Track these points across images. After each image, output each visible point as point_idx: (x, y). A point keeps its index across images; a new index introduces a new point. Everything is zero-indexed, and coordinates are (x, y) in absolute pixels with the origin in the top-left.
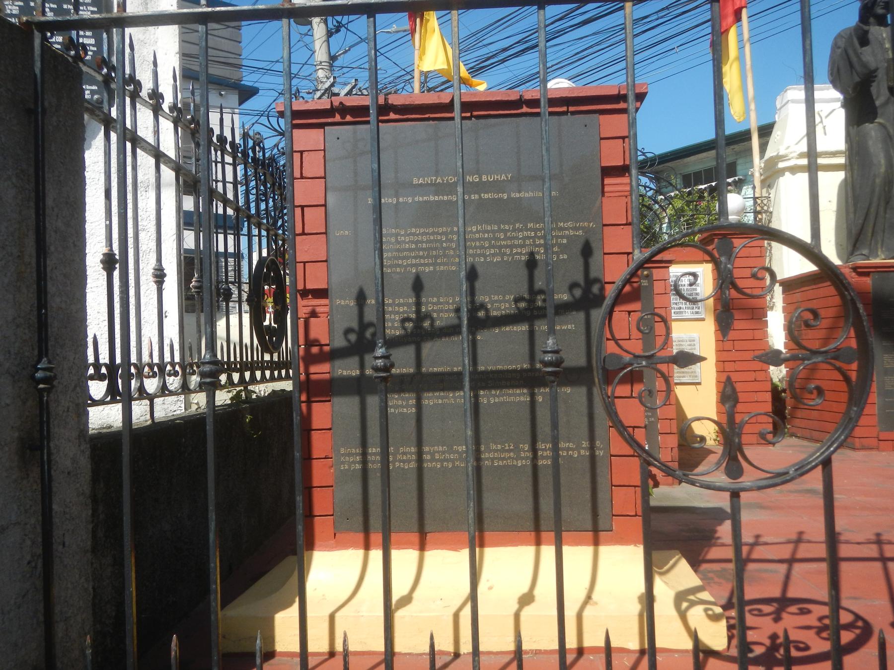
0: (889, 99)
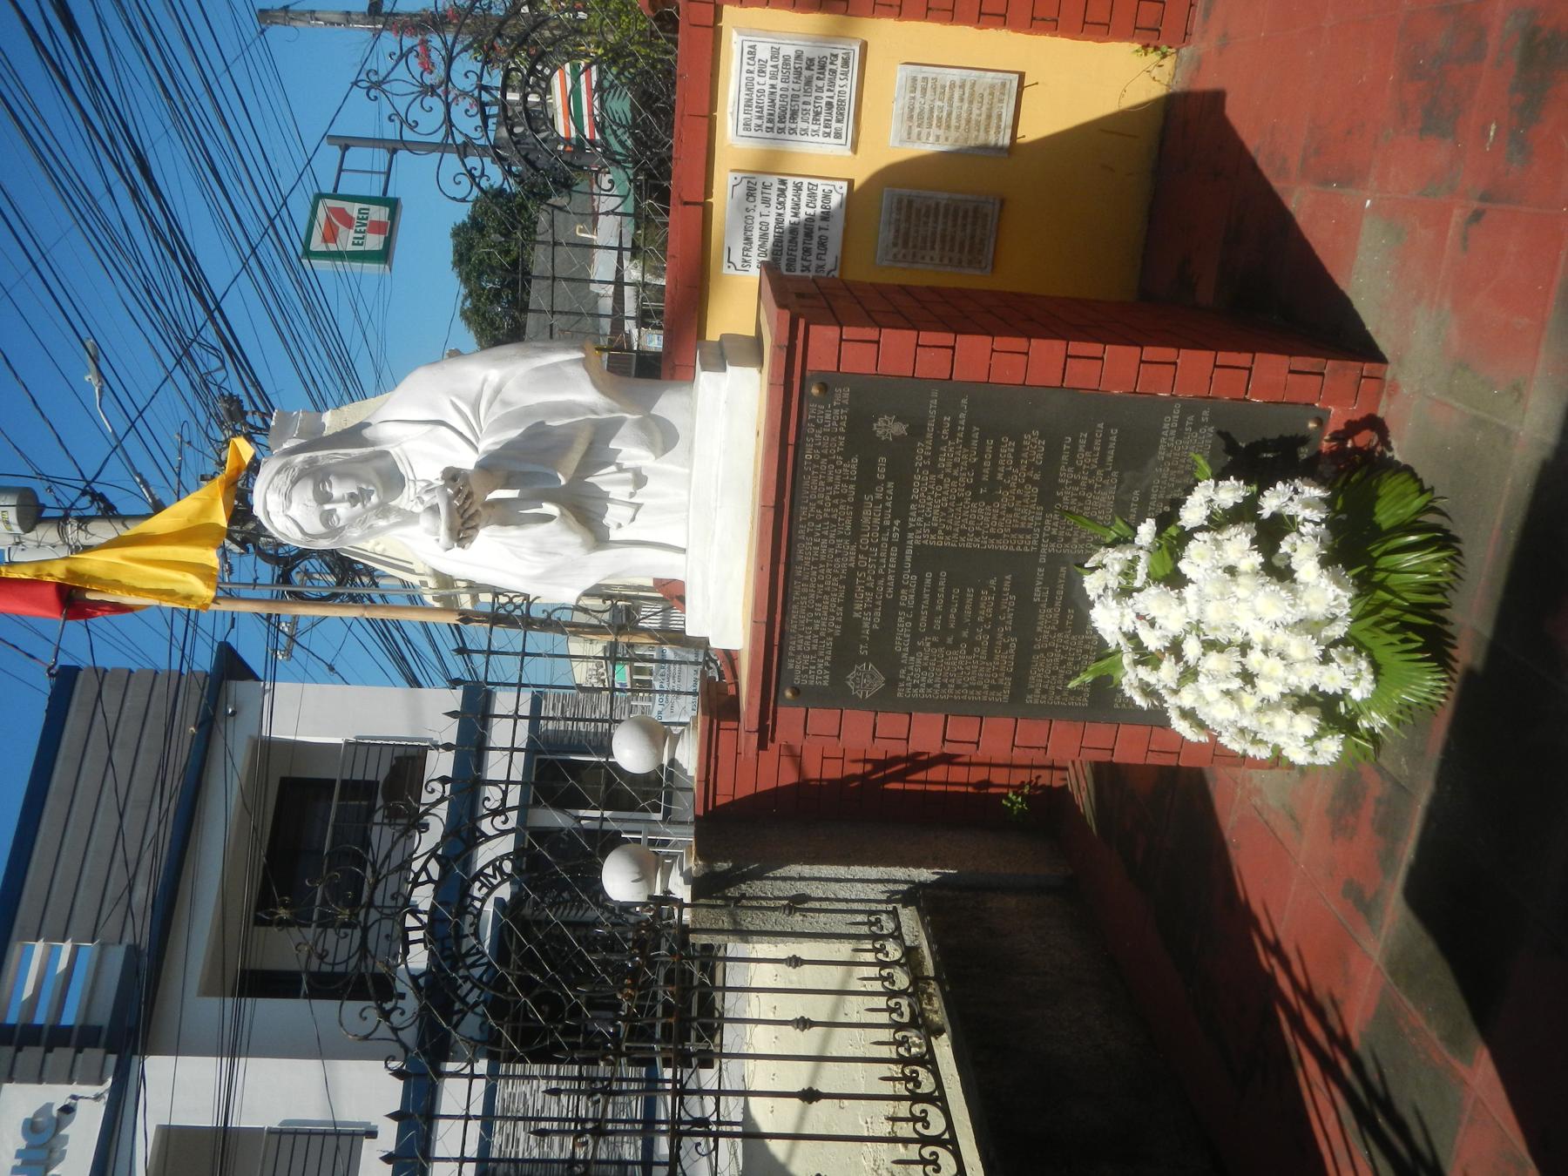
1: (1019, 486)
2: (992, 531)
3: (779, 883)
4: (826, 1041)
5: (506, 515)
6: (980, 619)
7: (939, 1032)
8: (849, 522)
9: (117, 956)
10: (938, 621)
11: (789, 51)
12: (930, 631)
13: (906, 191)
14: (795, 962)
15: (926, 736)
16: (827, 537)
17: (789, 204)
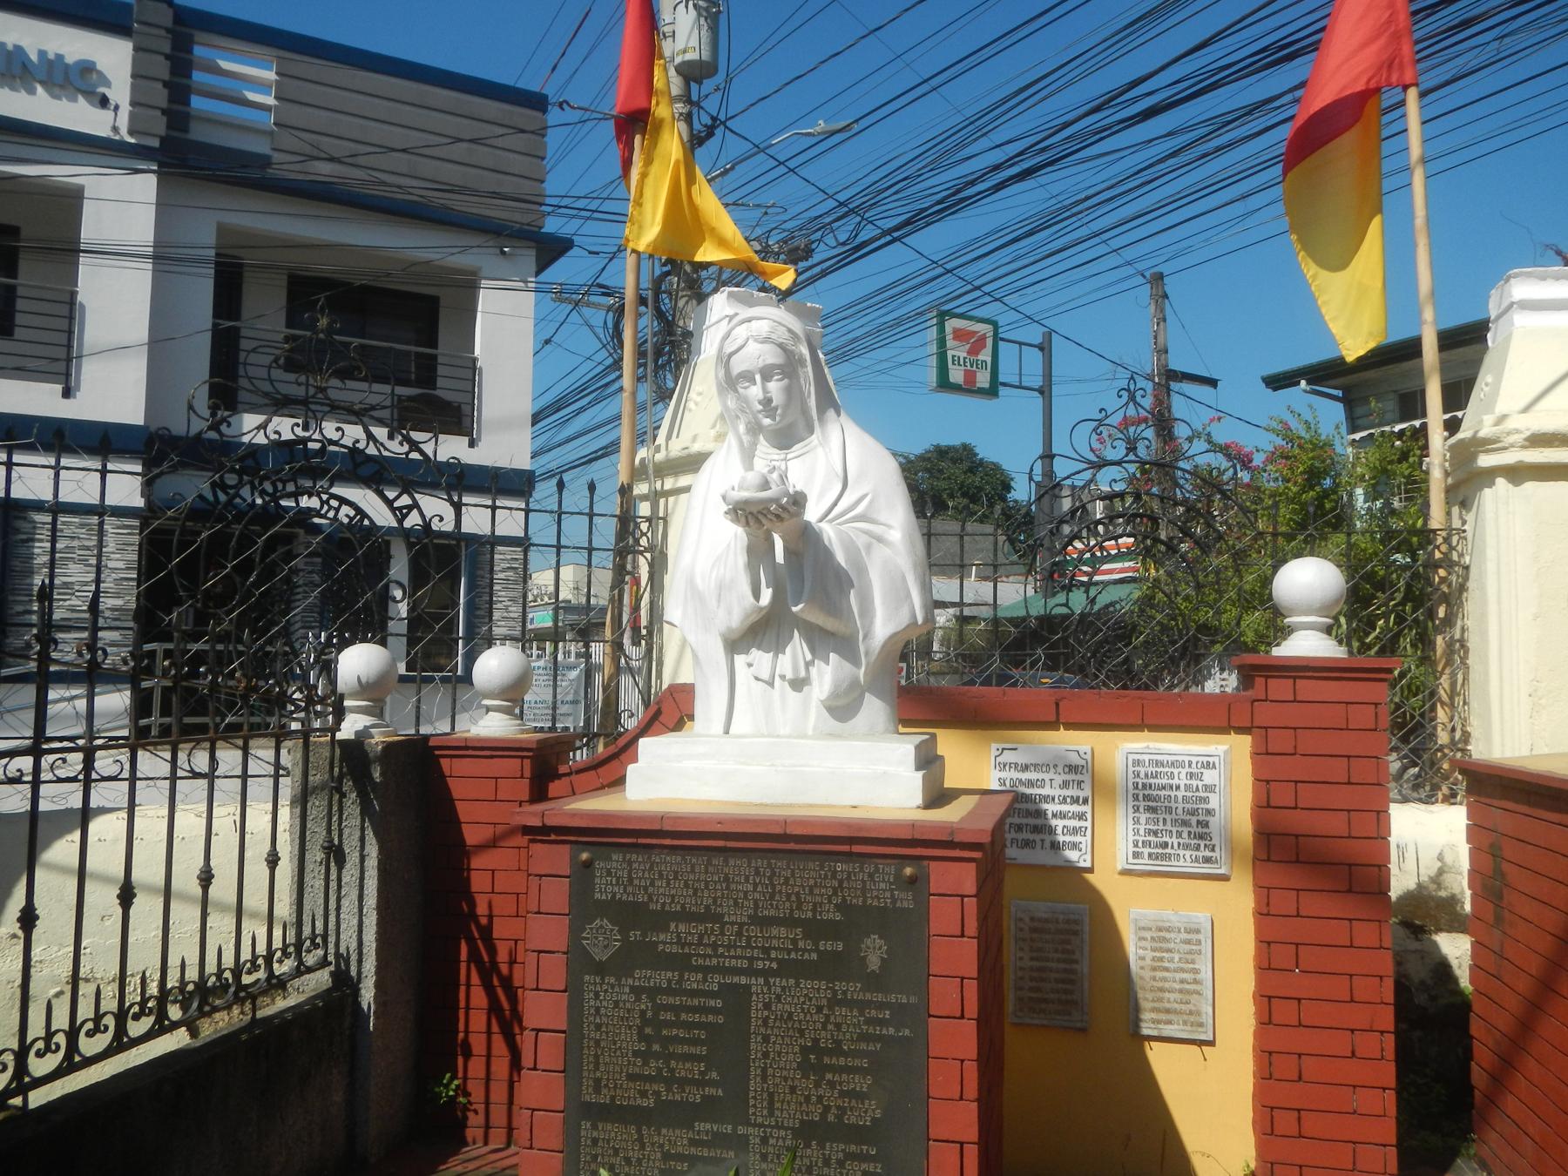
1: (820, 1098)
2: (770, 1071)
3: (358, 834)
4: (186, 898)
5: (758, 553)
6: (673, 1064)
7: (194, 1033)
8: (772, 913)
9: (260, 146)
10: (669, 1016)
11: (1214, 803)
12: (658, 1008)
13: (1087, 928)
14: (273, 860)
15: (542, 1010)
16: (755, 890)
17: (1065, 808)
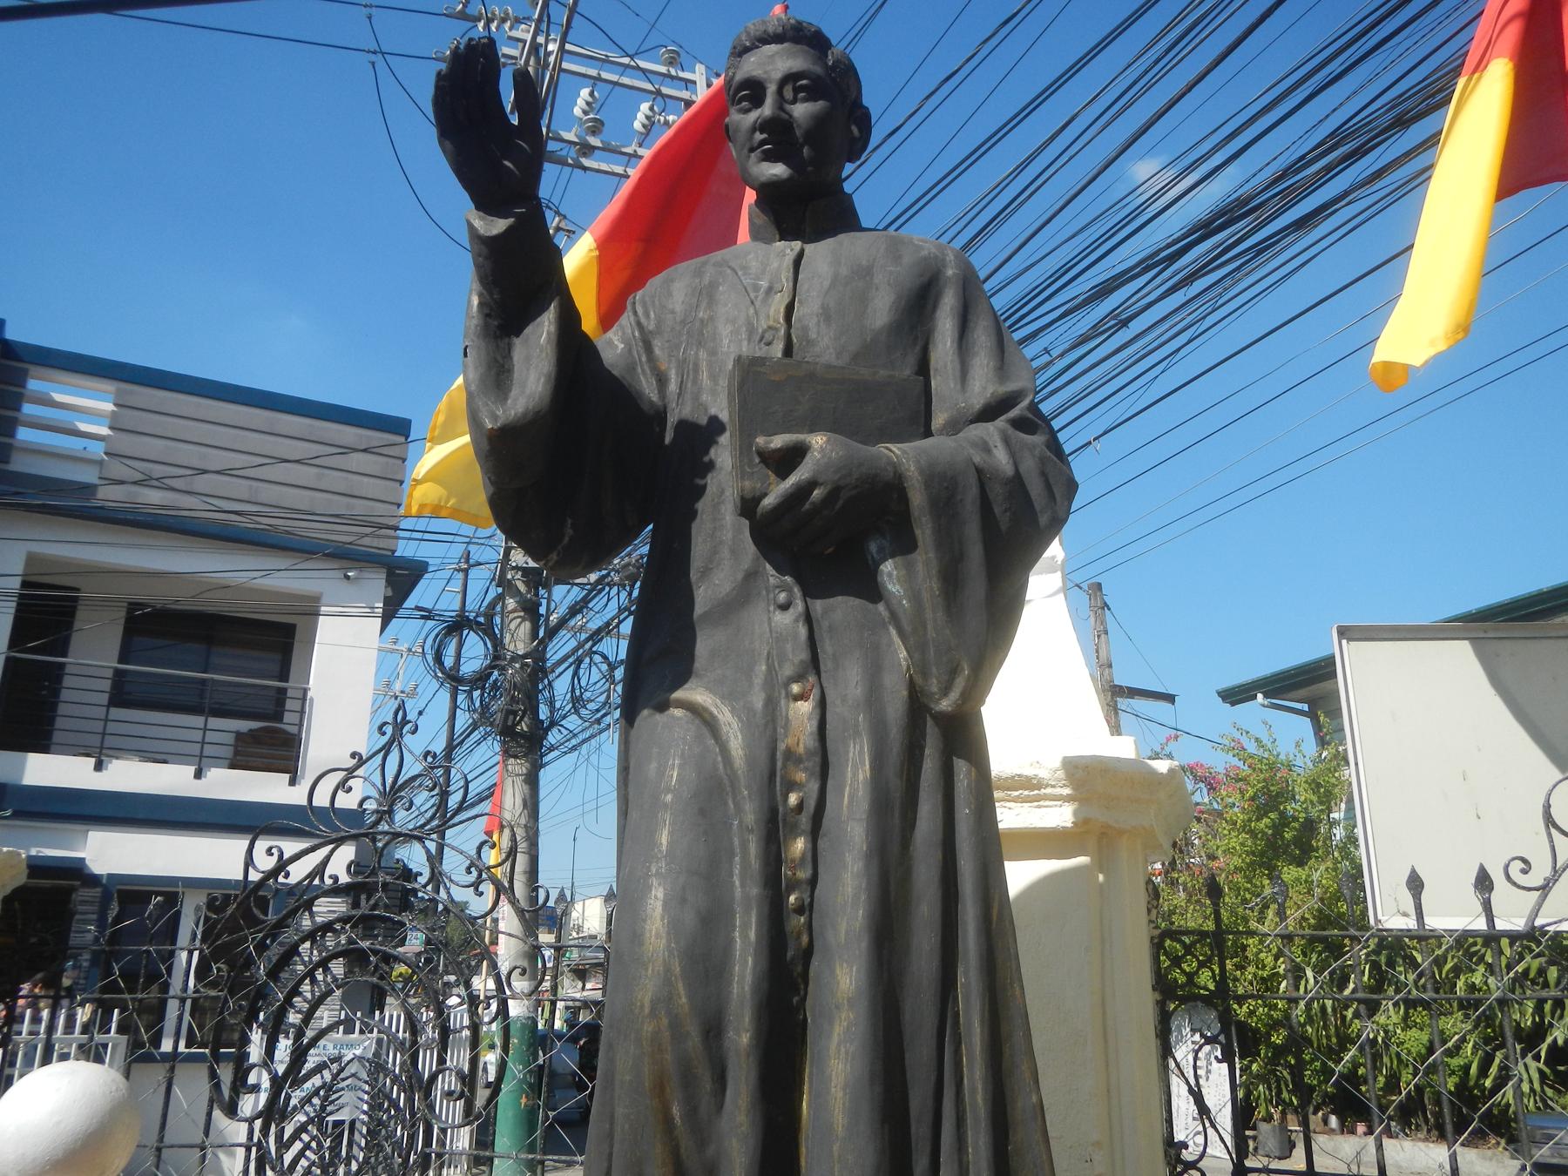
0: (752, 576)
9: (88, 476)
